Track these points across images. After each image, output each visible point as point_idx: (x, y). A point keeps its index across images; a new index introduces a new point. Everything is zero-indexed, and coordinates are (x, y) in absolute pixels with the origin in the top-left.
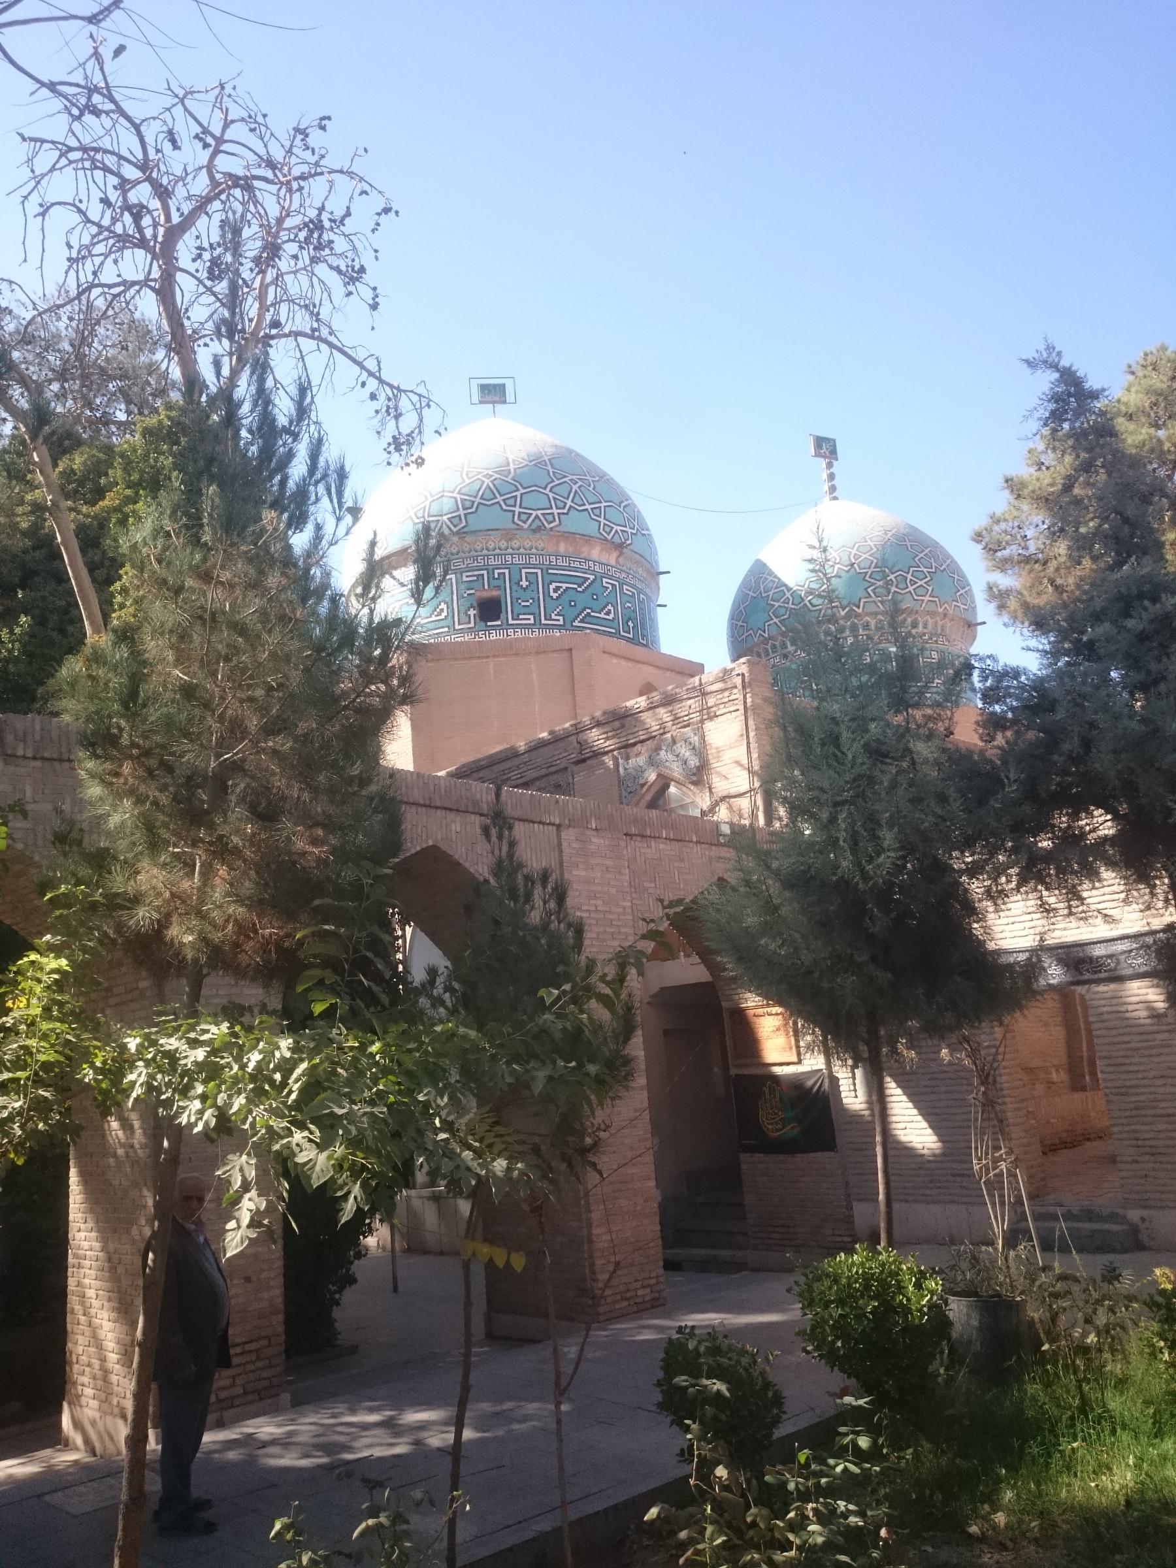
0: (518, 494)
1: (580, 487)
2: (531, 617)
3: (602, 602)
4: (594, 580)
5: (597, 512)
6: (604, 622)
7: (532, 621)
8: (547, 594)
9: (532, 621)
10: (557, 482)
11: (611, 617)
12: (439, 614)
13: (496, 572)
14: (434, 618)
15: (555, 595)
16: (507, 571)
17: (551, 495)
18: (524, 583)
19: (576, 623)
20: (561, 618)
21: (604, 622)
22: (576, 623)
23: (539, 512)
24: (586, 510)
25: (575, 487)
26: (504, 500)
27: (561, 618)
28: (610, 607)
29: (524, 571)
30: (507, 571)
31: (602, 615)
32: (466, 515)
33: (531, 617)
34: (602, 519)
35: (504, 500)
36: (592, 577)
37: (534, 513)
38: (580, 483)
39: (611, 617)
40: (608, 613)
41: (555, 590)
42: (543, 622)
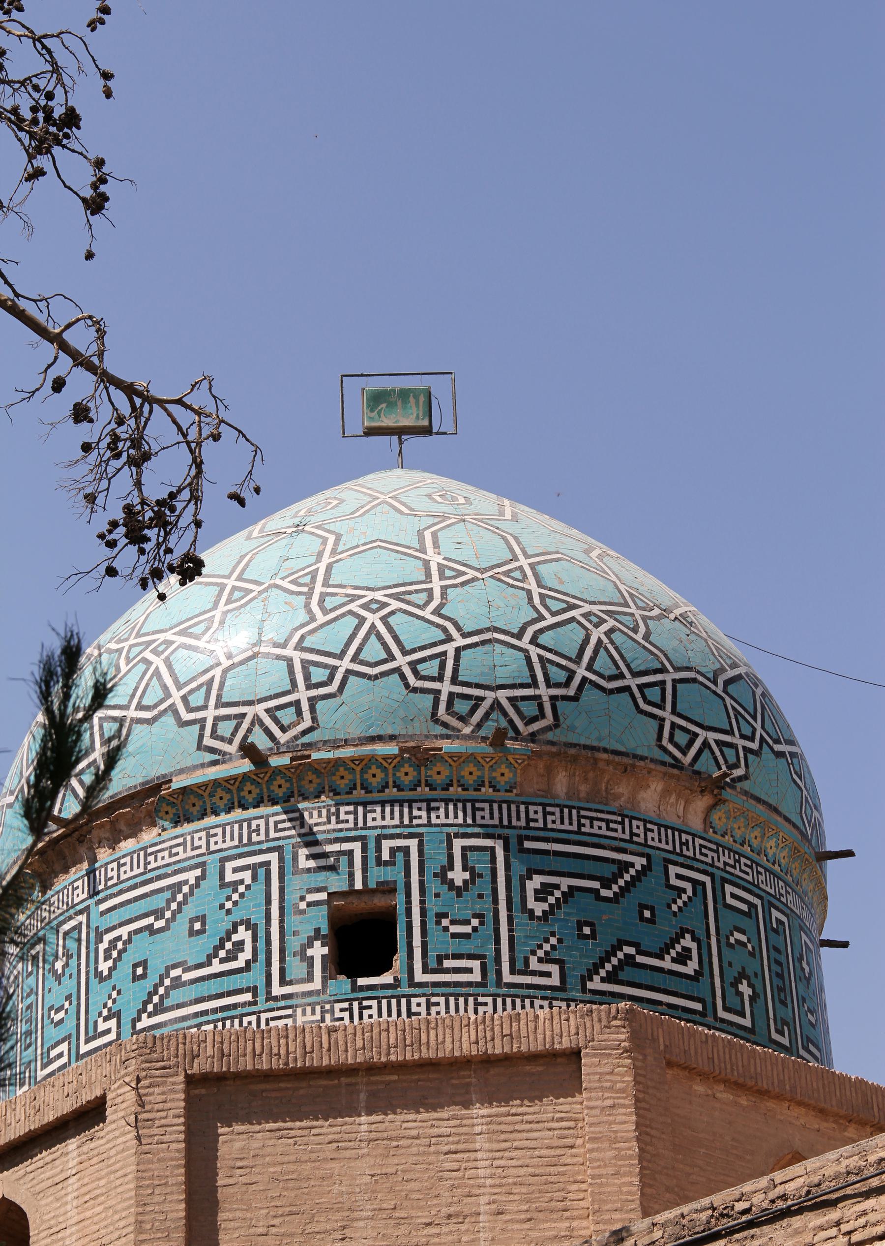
0: (450, 648)
1: (609, 633)
2: (476, 964)
3: (666, 928)
4: (646, 870)
5: (654, 694)
6: (673, 984)
7: (476, 977)
8: (514, 905)
9: (476, 977)
10: (551, 620)
11: (691, 967)
12: (231, 957)
13: (386, 845)
14: (217, 967)
15: (539, 908)
16: (413, 843)
17: (534, 652)
18: (458, 876)
19: (595, 984)
20: (554, 969)
21: (673, 984)
22: (595, 984)
23: (502, 695)
24: (627, 689)
25: (597, 634)
26: (413, 665)
27: (554, 969)
28: (687, 942)
29: (458, 844)
30: (413, 843)
31: (667, 964)
32: (312, 701)
33: (476, 964)
34: (667, 714)
35: (413, 665)
36: (639, 862)
37: (490, 695)
38: (611, 623)
39: (691, 967)
40: (683, 958)
41: (542, 894)
42: (507, 978)
